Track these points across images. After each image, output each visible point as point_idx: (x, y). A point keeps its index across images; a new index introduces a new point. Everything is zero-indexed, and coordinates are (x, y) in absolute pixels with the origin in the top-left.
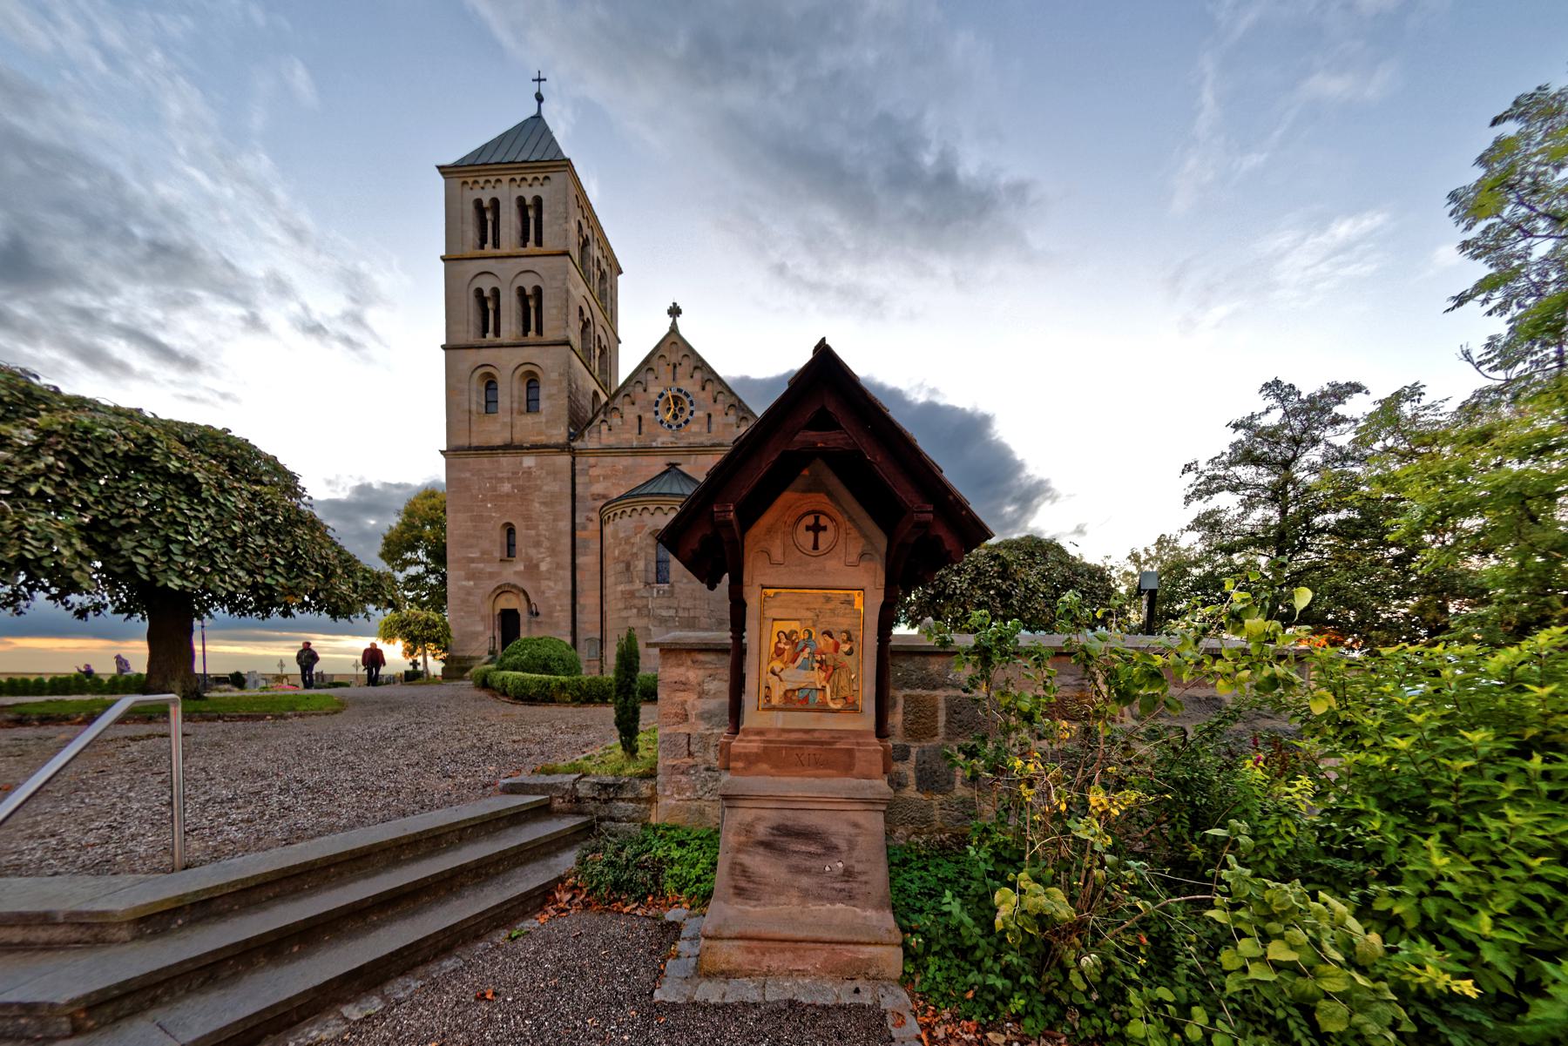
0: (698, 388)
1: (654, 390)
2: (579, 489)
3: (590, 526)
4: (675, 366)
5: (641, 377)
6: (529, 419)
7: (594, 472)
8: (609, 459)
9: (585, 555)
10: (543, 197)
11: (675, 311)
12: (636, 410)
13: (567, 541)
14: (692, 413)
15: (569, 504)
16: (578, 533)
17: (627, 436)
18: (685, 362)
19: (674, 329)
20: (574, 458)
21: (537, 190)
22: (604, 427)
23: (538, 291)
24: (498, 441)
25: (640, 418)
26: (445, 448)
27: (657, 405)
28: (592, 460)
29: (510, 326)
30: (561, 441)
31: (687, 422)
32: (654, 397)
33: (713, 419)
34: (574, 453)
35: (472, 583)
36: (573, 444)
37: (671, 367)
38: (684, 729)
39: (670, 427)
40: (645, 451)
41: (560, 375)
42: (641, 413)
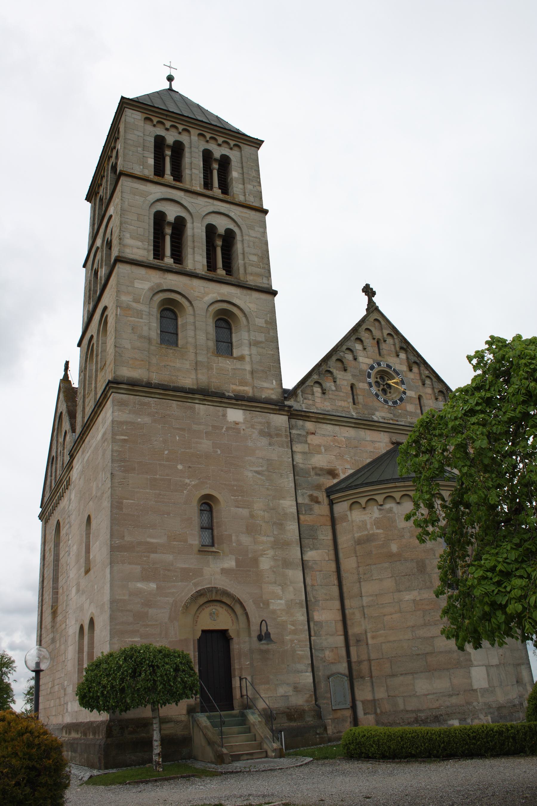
1: (365, 361)
3: (316, 508)
5: (349, 344)
6: (226, 364)
8: (329, 428)
9: (314, 548)
19: (372, 308)
25: (352, 387)
28: (309, 426)
30: (274, 397)
35: (153, 586)
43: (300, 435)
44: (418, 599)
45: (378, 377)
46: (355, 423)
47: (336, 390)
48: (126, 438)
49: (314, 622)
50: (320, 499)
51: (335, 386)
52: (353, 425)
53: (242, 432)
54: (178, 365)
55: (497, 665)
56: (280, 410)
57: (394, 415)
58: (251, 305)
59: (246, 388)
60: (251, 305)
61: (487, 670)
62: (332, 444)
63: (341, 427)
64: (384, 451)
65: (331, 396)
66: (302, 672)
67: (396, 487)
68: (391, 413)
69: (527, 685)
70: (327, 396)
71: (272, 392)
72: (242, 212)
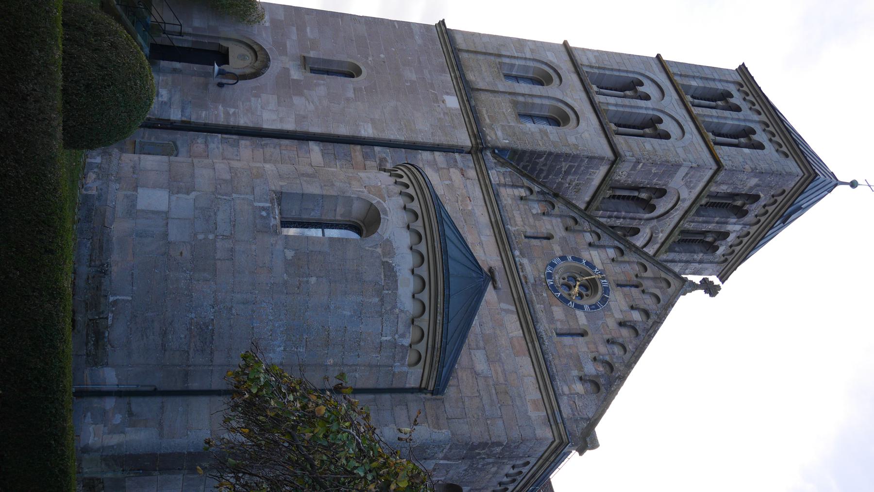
0: (619, 316)
7: (455, 174)
12: (559, 232)
13: (343, 130)
17: (519, 220)
25: (549, 237)
28: (472, 173)
30: (489, 138)
36: (488, 153)
42: (557, 238)
46: (496, 221)
47: (533, 215)
49: (238, 140)
51: (538, 214)
52: (493, 220)
54: (484, 69)
55: (166, 235)
56: (475, 136)
57: (534, 285)
59: (488, 121)
61: (163, 212)
63: (485, 207)
65: (521, 206)
66: (182, 111)
69: (123, 435)
70: (519, 202)
72: (699, 144)
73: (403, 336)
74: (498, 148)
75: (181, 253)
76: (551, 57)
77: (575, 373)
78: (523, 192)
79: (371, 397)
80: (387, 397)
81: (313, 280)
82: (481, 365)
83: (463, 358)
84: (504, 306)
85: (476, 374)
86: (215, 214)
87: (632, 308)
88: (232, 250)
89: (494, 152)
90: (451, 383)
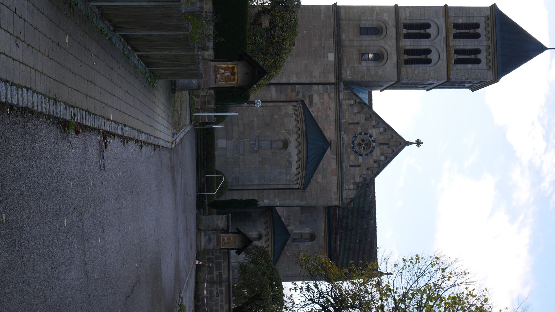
0: (375, 158)
1: (374, 132)
2: (316, 87)
3: (294, 94)
4: (388, 144)
8: (333, 105)
9: (276, 91)
10: (480, 65)
11: (419, 143)
12: (363, 121)
14: (361, 155)
15: (307, 82)
16: (290, 86)
18: (390, 151)
19: (409, 143)
20: (333, 84)
21: (484, 61)
22: (352, 102)
23: (428, 62)
24: (344, 37)
25: (358, 123)
26: (338, 4)
27: (366, 134)
28: (333, 95)
29: (409, 44)
30: (343, 76)
31: (356, 152)
32: (370, 132)
33: (358, 168)
34: (336, 84)
37: (387, 142)
38: (215, 220)
39: (353, 142)
40: (339, 127)
41: (381, 76)
42: (361, 124)
43: (327, 89)
44: (254, 122)
45: (367, 142)
46: (337, 120)
47: (354, 113)
48: (314, 10)
50: (298, 97)
51: (356, 112)
53: (324, 60)
55: (226, 155)
56: (337, 78)
57: (346, 146)
58: (389, 68)
59: (345, 64)
60: (389, 68)
62: (325, 106)
63: (335, 112)
64: (325, 135)
67: (302, 118)
68: (347, 144)
71: (345, 76)
73: (293, 178)
74: (346, 82)
75: (230, 161)
76: (386, 17)
77: (352, 181)
78: (352, 102)
79: (283, 190)
80: (288, 190)
81: (267, 166)
82: (320, 179)
83: (314, 177)
84: (333, 156)
85: (317, 182)
86: (239, 147)
87: (381, 155)
88: (244, 159)
89: (344, 83)
90: (308, 186)
